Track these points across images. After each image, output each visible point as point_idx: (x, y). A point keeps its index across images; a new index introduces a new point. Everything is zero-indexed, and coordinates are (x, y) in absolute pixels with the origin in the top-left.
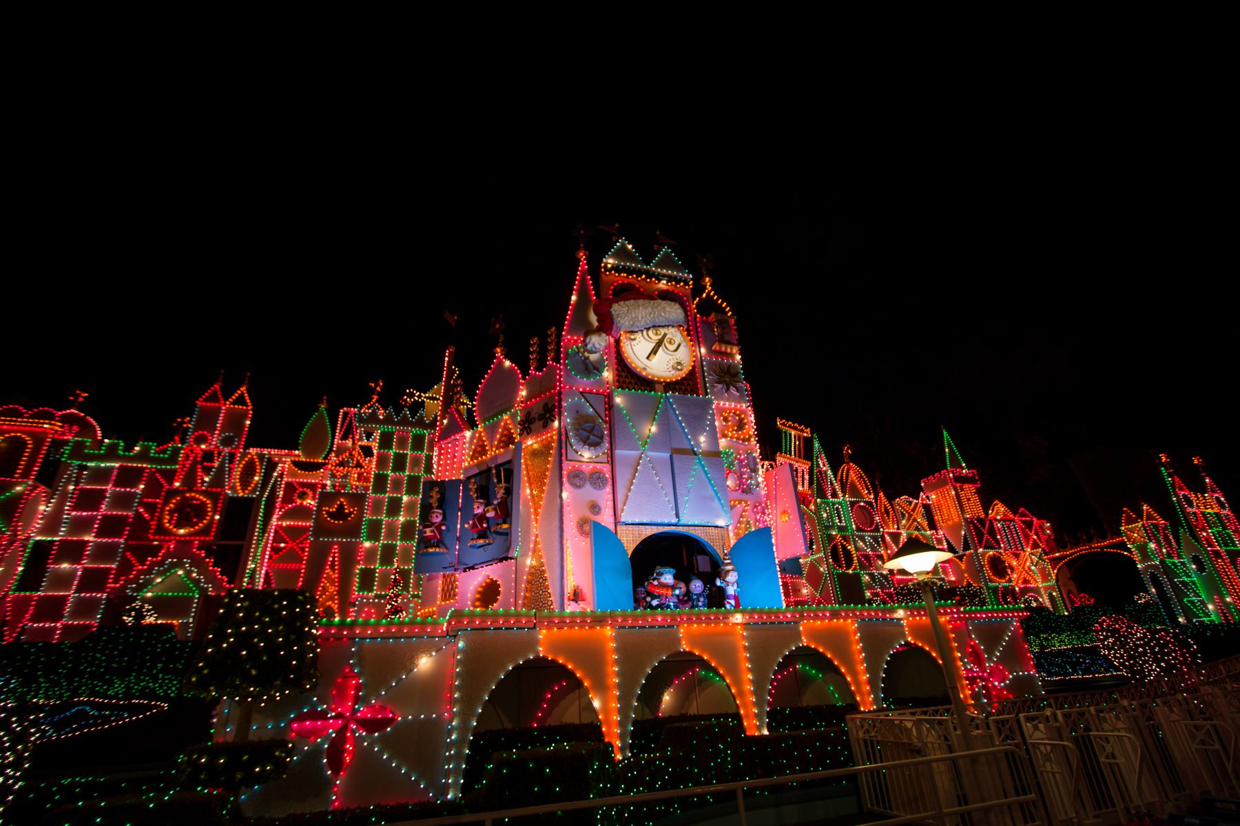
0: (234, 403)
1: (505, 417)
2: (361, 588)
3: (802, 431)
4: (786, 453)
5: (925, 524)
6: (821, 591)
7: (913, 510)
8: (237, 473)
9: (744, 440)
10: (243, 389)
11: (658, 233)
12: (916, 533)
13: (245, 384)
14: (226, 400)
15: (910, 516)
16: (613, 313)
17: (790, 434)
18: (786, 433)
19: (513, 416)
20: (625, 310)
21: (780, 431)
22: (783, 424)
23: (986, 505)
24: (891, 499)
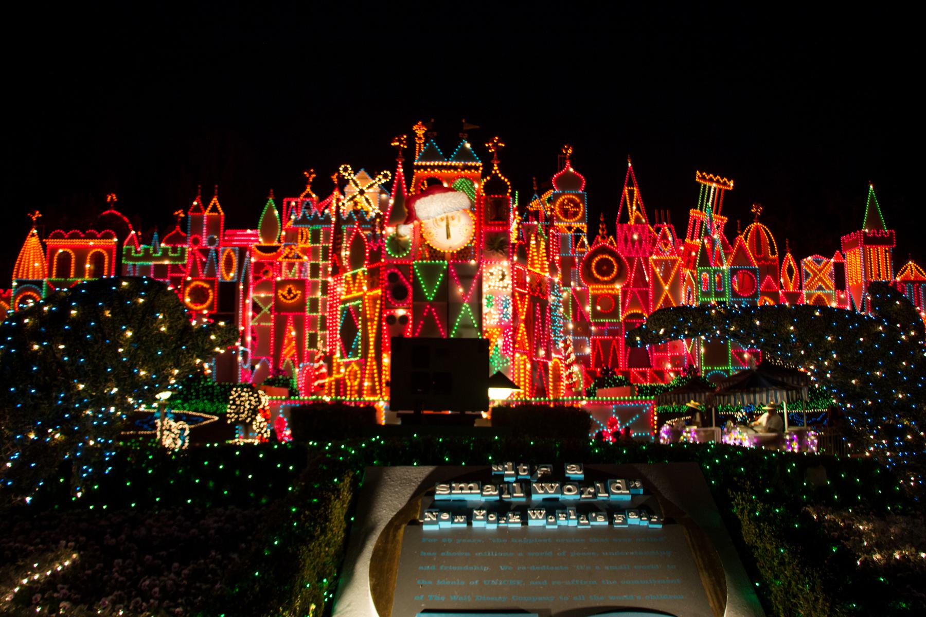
0: (210, 211)
1: (359, 271)
2: (310, 347)
3: (725, 184)
4: (701, 209)
5: (831, 283)
6: (692, 349)
7: (820, 271)
8: (222, 264)
9: (504, 287)
10: (215, 199)
11: (464, 121)
12: (819, 292)
13: (215, 195)
14: (206, 209)
15: (815, 275)
16: (416, 208)
17: (710, 188)
18: (705, 186)
19: (363, 272)
20: (423, 206)
21: (699, 184)
22: (703, 178)
23: (897, 267)
24: (798, 260)
